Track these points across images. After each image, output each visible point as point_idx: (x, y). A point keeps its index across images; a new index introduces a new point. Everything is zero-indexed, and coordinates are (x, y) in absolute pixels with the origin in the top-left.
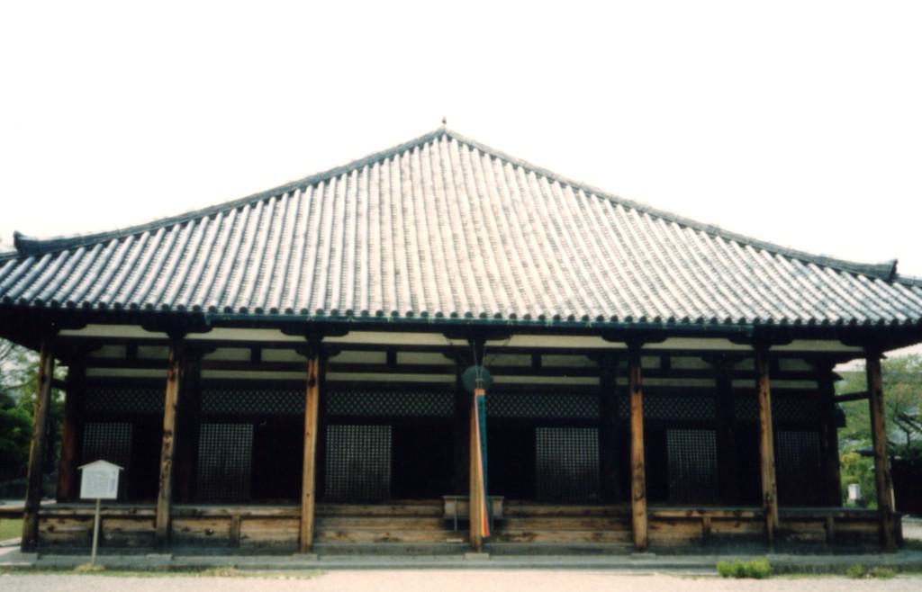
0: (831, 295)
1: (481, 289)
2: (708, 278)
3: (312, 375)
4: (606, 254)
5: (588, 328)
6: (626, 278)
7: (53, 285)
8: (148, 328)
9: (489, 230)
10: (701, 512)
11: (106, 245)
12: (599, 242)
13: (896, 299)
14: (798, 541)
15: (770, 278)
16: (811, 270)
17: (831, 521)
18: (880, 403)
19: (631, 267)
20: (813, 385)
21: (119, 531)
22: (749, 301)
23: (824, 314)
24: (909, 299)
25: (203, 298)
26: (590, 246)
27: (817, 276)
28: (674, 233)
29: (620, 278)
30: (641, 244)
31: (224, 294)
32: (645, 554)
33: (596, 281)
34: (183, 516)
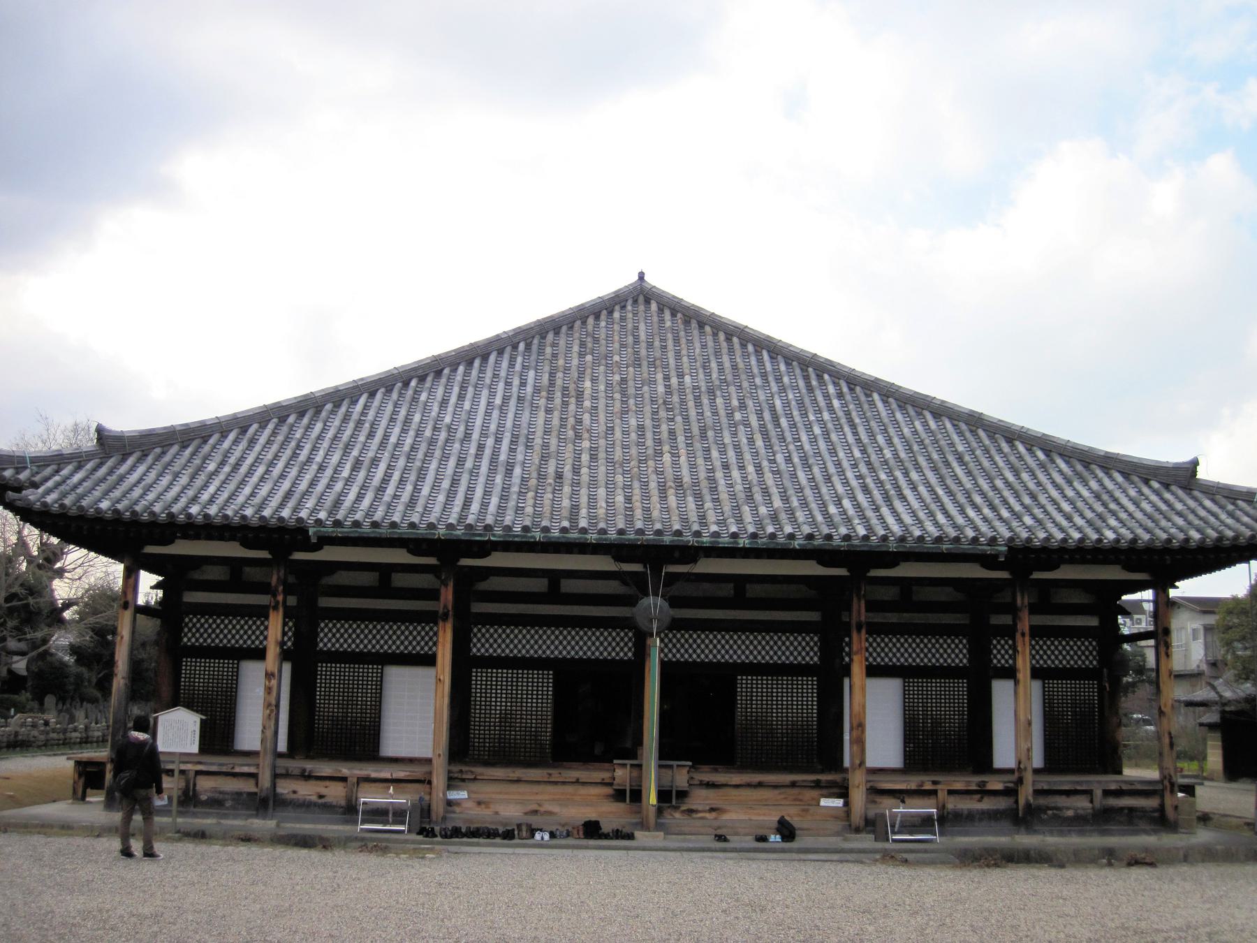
0: (1113, 506)
1: (663, 497)
2: (960, 483)
3: (445, 606)
4: (833, 452)
5: (794, 550)
7: (137, 492)
8: (246, 544)
9: (686, 419)
10: (935, 783)
11: (205, 440)
12: (826, 434)
13: (1193, 512)
14: (1055, 817)
15: (1039, 484)
16: (1093, 473)
17: (1098, 793)
18: (1168, 645)
19: (863, 469)
20: (1093, 622)
21: (215, 790)
22: (1005, 514)
23: (1098, 531)
24: (1209, 511)
25: (310, 511)
26: (813, 440)
27: (1100, 482)
28: (925, 424)
29: (846, 483)
30: (880, 439)
31: (337, 503)
32: (863, 835)
33: (816, 488)
34: (287, 775)
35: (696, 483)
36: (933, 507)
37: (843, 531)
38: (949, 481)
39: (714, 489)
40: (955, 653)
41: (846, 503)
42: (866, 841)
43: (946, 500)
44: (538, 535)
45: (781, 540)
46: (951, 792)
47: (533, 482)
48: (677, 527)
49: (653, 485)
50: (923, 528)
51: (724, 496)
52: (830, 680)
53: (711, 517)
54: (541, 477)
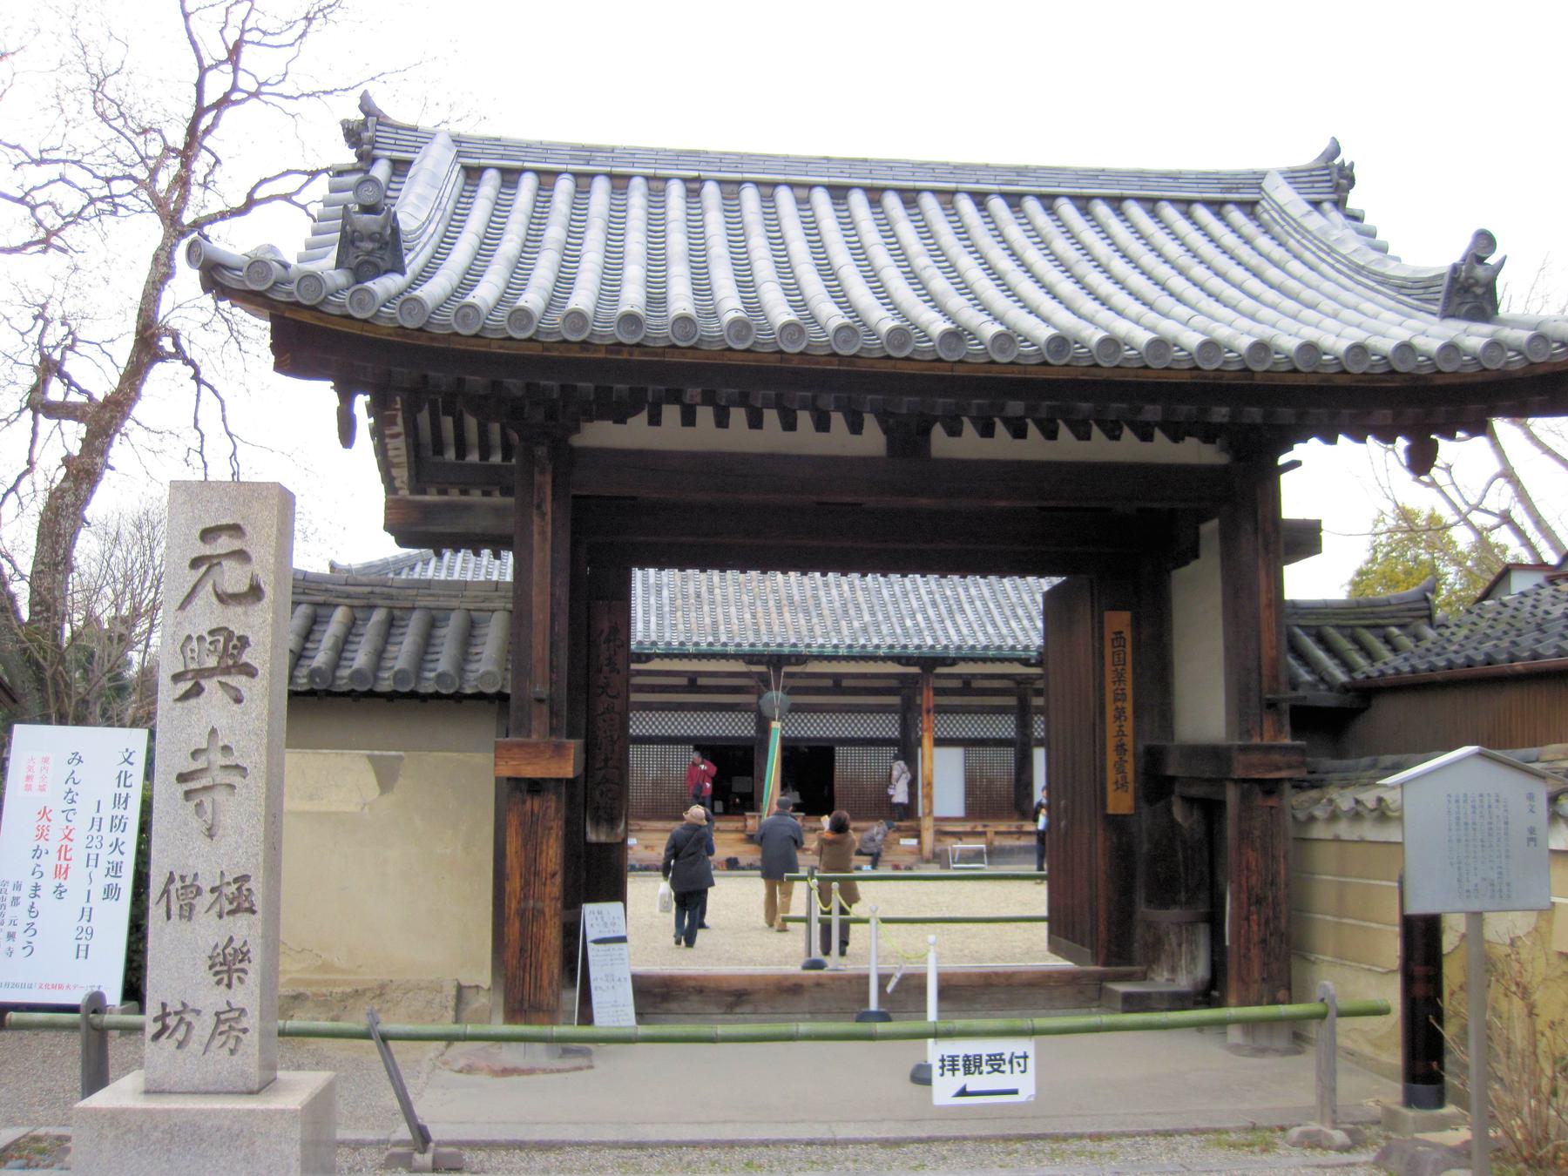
1: (780, 614)
2: (1008, 598)
6: (926, 598)
29: (919, 599)
35: (804, 601)
36: (985, 619)
37: (916, 641)
38: (1000, 597)
39: (818, 605)
40: (1006, 727)
41: (919, 617)
42: (934, 870)
43: (995, 612)
44: (691, 649)
45: (870, 649)
46: (997, 833)
47: (679, 602)
48: (793, 640)
49: (771, 603)
50: (976, 639)
51: (826, 612)
52: (907, 749)
53: (818, 631)
54: (685, 597)
